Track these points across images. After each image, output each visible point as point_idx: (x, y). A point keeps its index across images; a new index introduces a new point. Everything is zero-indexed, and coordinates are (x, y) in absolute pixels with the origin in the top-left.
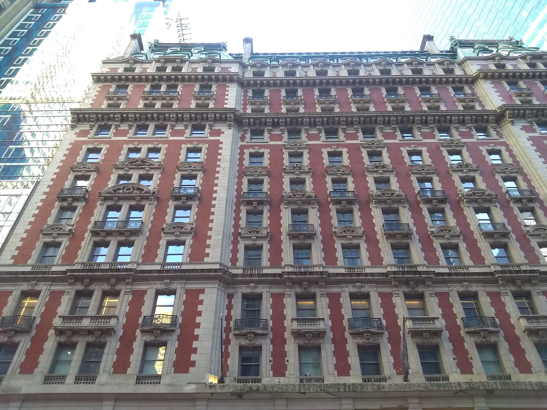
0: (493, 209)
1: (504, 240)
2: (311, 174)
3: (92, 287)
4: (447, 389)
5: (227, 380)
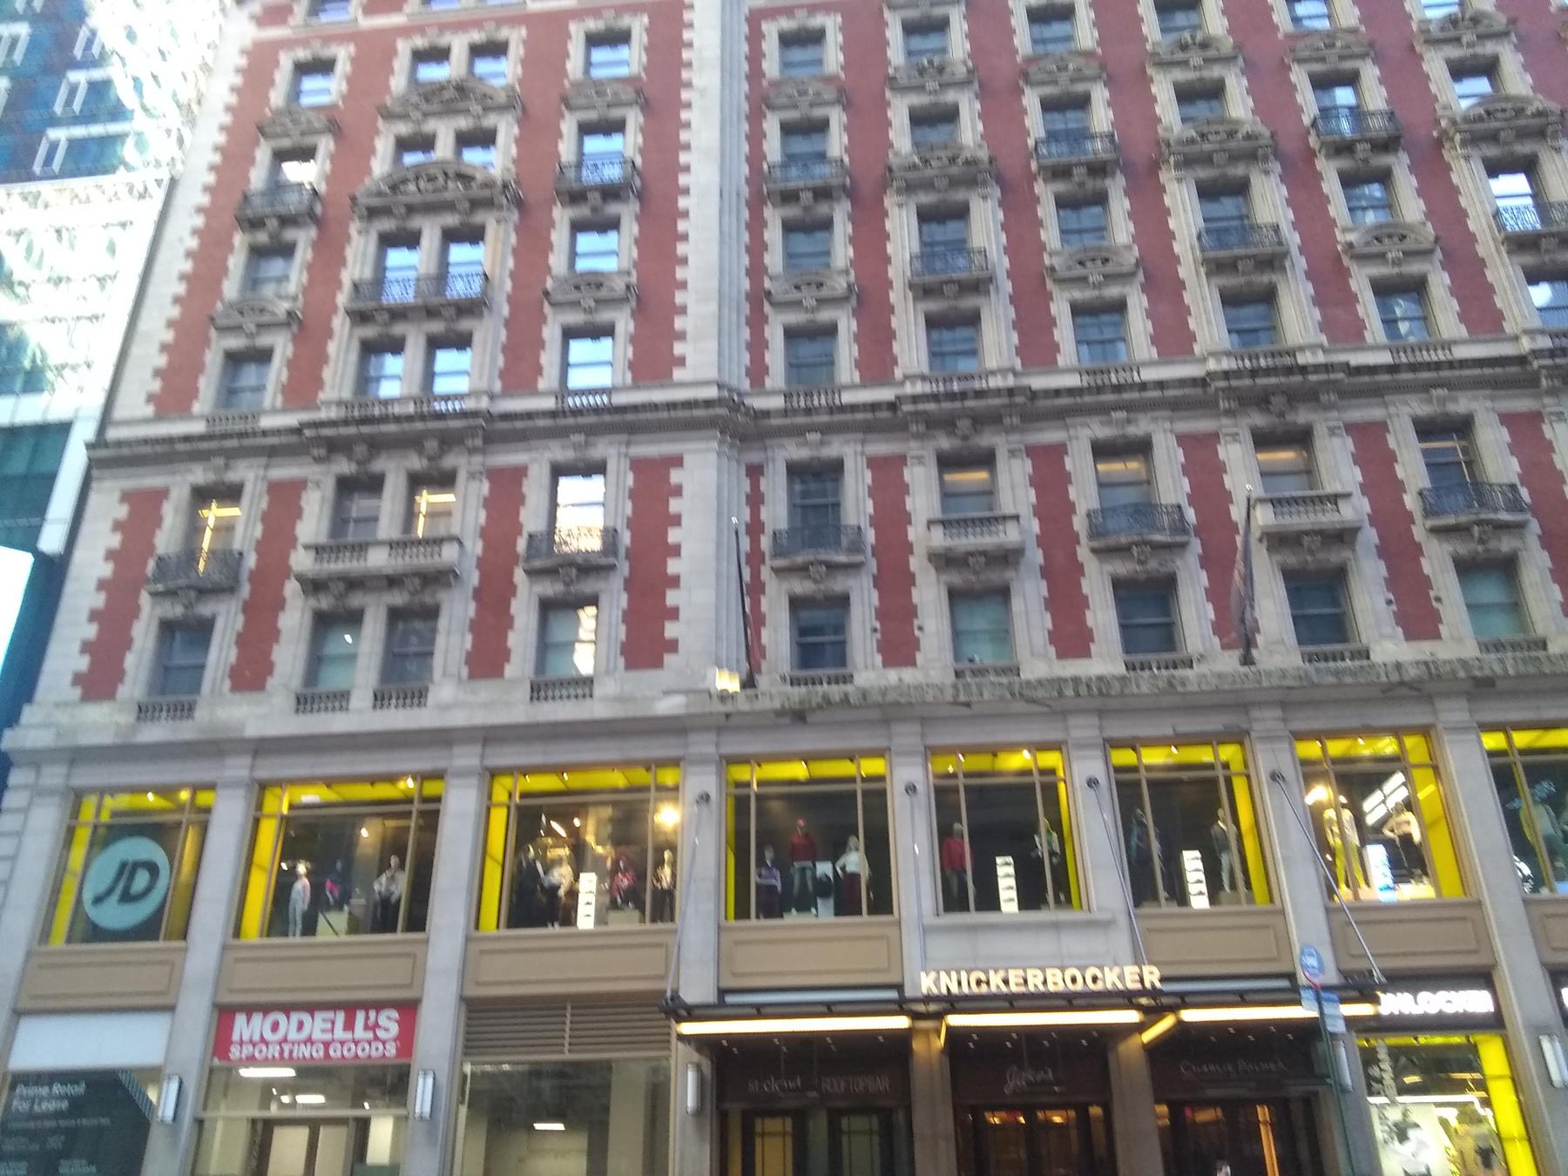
2: (976, 86)
3: (378, 465)
4: (1362, 680)
5: (763, 681)
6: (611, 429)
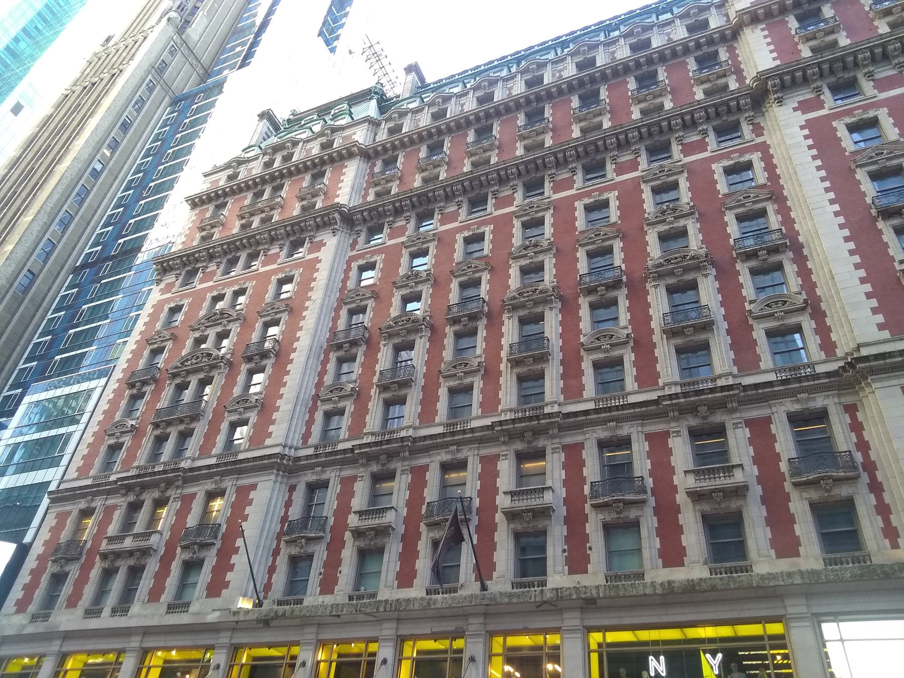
1: (702, 337)
4: (522, 600)
5: (266, 602)
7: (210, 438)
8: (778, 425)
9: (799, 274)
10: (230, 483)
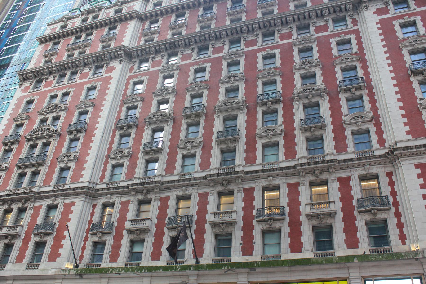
0: (320, 102)
1: (319, 133)
6: (61, 195)
7: (49, 176)
8: (354, 181)
9: (370, 102)
10: (60, 201)
